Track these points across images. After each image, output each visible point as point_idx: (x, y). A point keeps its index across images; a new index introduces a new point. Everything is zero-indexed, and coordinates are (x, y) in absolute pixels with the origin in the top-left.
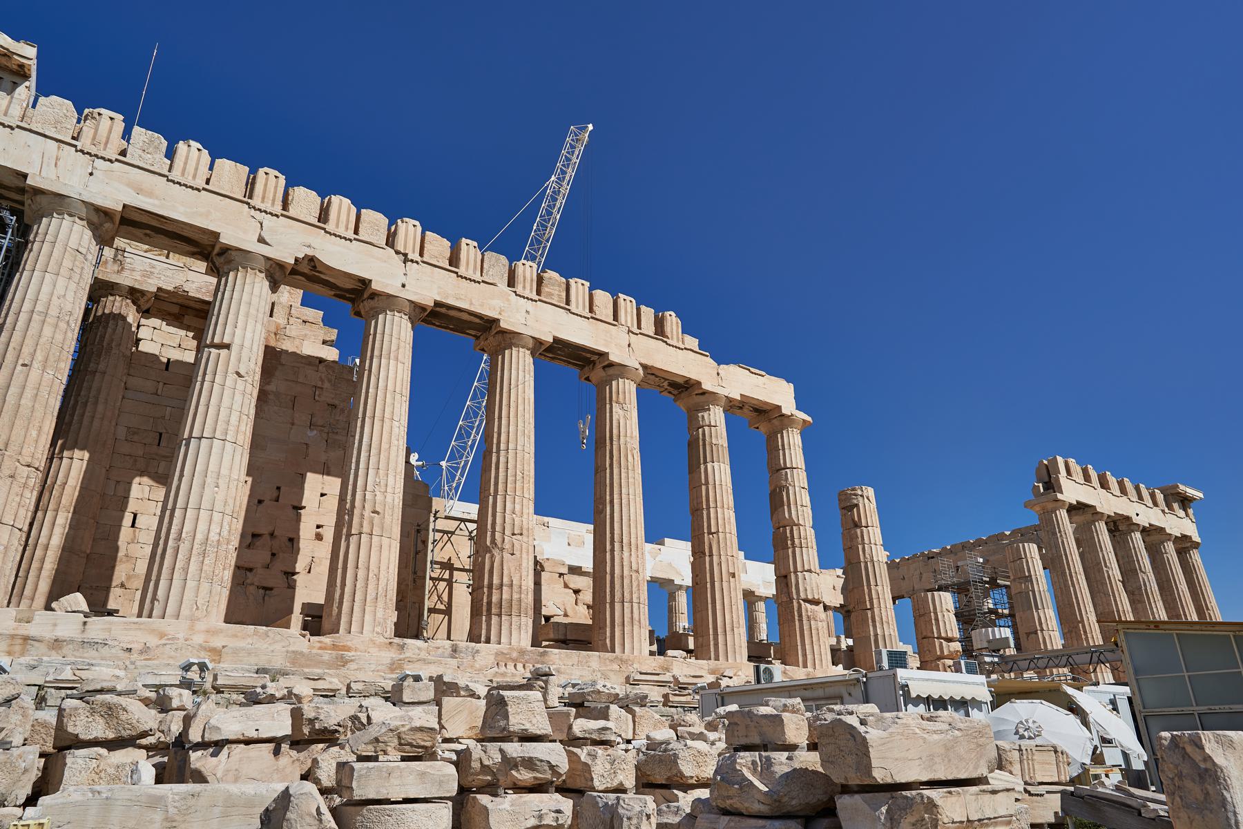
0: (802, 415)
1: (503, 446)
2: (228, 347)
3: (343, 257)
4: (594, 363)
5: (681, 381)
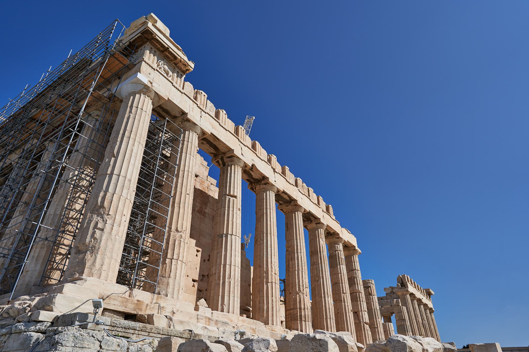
0: (360, 251)
1: (299, 251)
2: (236, 197)
3: (264, 169)
4: (311, 221)
5: (332, 232)
